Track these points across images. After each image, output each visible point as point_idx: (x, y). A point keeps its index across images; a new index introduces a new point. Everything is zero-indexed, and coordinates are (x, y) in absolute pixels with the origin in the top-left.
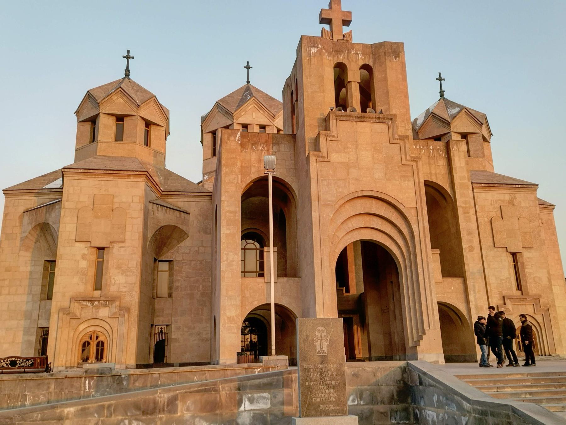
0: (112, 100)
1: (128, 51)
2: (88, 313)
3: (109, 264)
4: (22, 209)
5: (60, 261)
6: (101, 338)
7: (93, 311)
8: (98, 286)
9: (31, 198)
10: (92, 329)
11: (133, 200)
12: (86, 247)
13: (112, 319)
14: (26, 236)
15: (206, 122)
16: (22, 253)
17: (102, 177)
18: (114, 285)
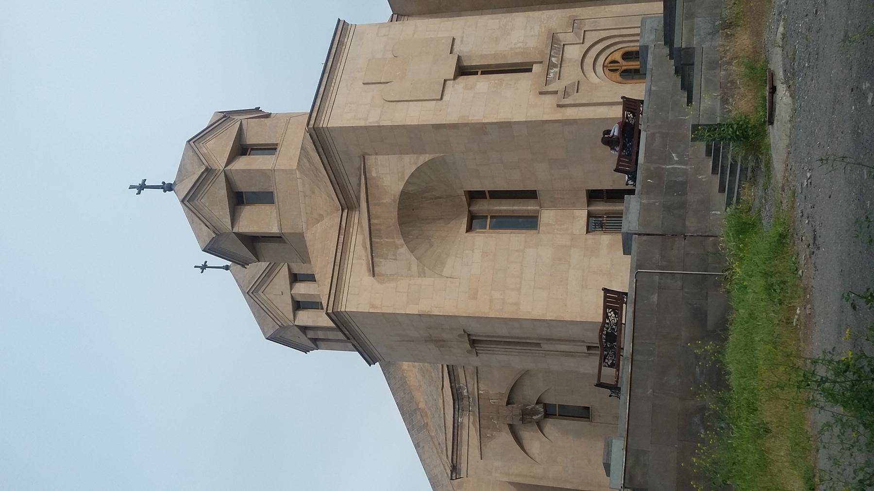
0: (208, 154)
1: (132, 187)
2: (570, 74)
3: (489, 53)
4: (368, 280)
5: (470, 118)
6: (618, 56)
7: (568, 66)
8: (524, 68)
9: (350, 265)
10: (599, 69)
11: (384, 36)
12: (453, 87)
13: (585, 40)
14: (417, 259)
15: (276, 318)
16: (446, 272)
17: (335, 77)
18: (527, 43)
